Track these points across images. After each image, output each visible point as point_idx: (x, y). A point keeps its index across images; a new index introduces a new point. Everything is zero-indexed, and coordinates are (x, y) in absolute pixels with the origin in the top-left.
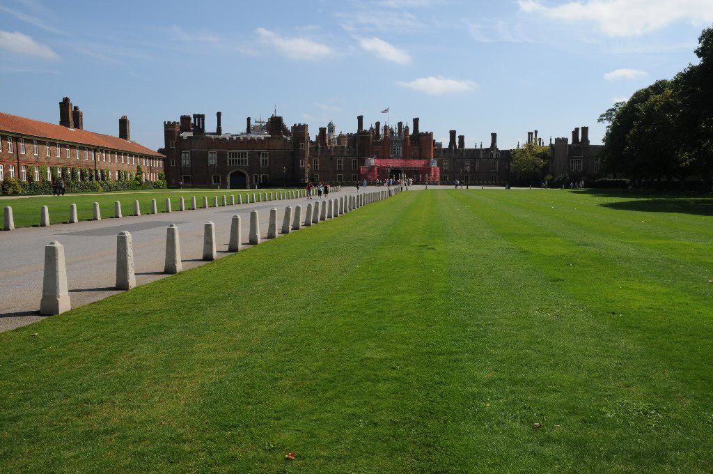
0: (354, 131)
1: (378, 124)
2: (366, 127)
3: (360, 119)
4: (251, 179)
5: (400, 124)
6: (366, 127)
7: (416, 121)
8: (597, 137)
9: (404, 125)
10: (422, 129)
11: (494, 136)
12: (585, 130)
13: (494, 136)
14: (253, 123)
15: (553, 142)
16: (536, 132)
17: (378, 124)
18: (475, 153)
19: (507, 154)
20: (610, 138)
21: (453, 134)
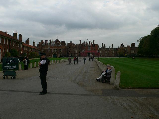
0: (79, 43)
1: (85, 42)
2: (82, 43)
3: (80, 41)
4: (58, 55)
5: (90, 42)
6: (82, 43)
7: (94, 41)
8: (137, 45)
9: (91, 42)
10: (95, 43)
11: (112, 45)
12: (134, 43)
13: (112, 45)
14: (51, 41)
15: (127, 46)
16: (123, 44)
17: (85, 42)
18: (108, 49)
19: (116, 49)
20: (139, 46)
21: (102, 44)
